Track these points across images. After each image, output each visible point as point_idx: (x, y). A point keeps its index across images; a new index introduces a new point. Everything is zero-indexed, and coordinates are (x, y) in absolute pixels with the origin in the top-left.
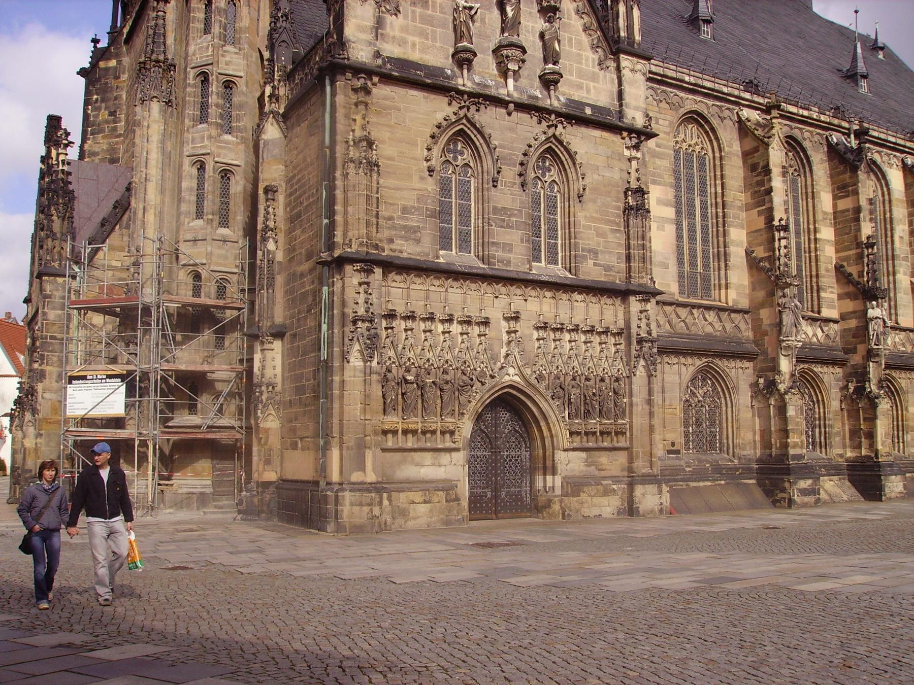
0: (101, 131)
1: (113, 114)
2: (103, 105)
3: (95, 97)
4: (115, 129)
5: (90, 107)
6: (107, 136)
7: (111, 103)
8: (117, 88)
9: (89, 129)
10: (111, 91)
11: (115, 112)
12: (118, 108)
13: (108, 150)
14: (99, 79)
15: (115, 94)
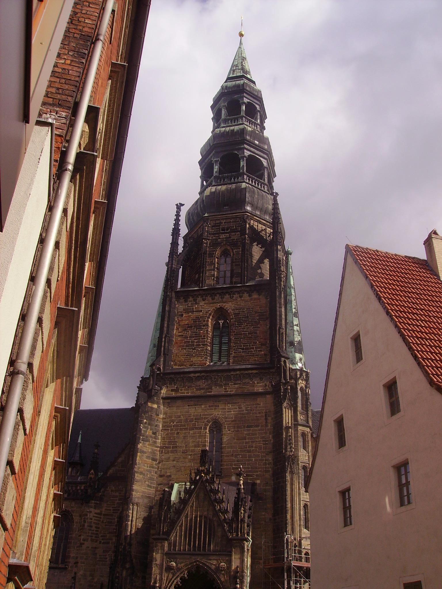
0: (149, 441)
1: (154, 433)
2: (149, 427)
3: (145, 421)
4: (155, 442)
5: (142, 425)
6: (151, 445)
7: (153, 427)
8: (157, 421)
9: (141, 437)
10: (154, 421)
11: (156, 433)
12: (158, 431)
13: (151, 453)
14: (147, 412)
15: (156, 423)
